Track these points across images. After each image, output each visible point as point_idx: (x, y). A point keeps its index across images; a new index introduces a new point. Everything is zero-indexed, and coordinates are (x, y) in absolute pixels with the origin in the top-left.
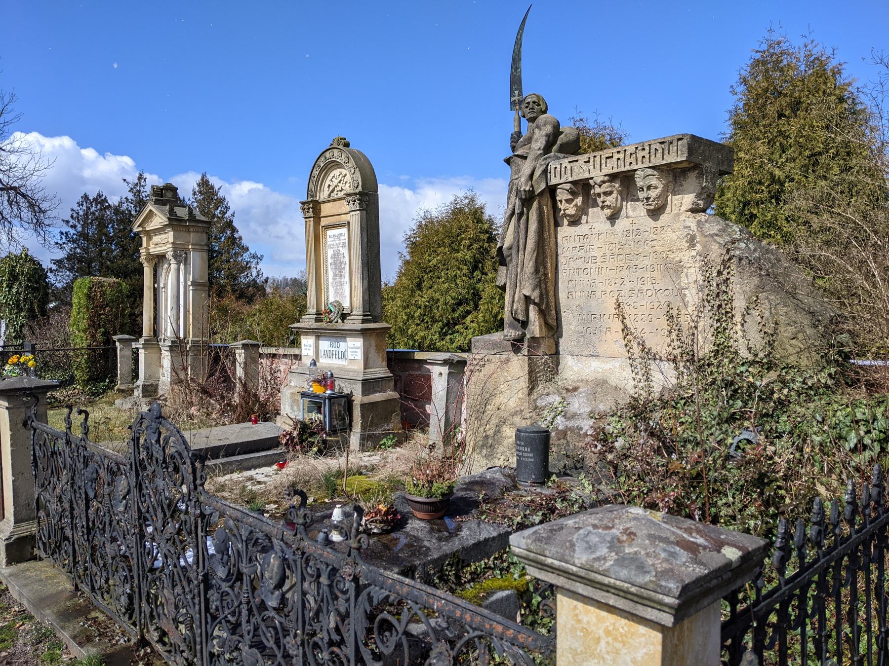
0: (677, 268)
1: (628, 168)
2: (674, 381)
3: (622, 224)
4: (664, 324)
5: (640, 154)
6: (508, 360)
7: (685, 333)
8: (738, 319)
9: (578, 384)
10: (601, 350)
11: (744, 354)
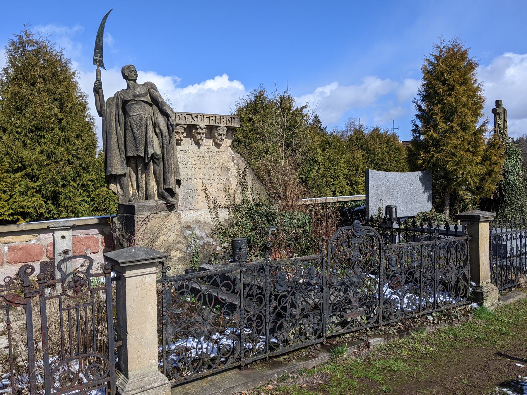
0: (227, 170)
1: (217, 124)
2: (228, 216)
3: (202, 148)
4: (223, 193)
5: (222, 120)
6: (167, 215)
7: (232, 195)
8: (249, 189)
9: (188, 224)
10: (195, 207)
11: (252, 202)
